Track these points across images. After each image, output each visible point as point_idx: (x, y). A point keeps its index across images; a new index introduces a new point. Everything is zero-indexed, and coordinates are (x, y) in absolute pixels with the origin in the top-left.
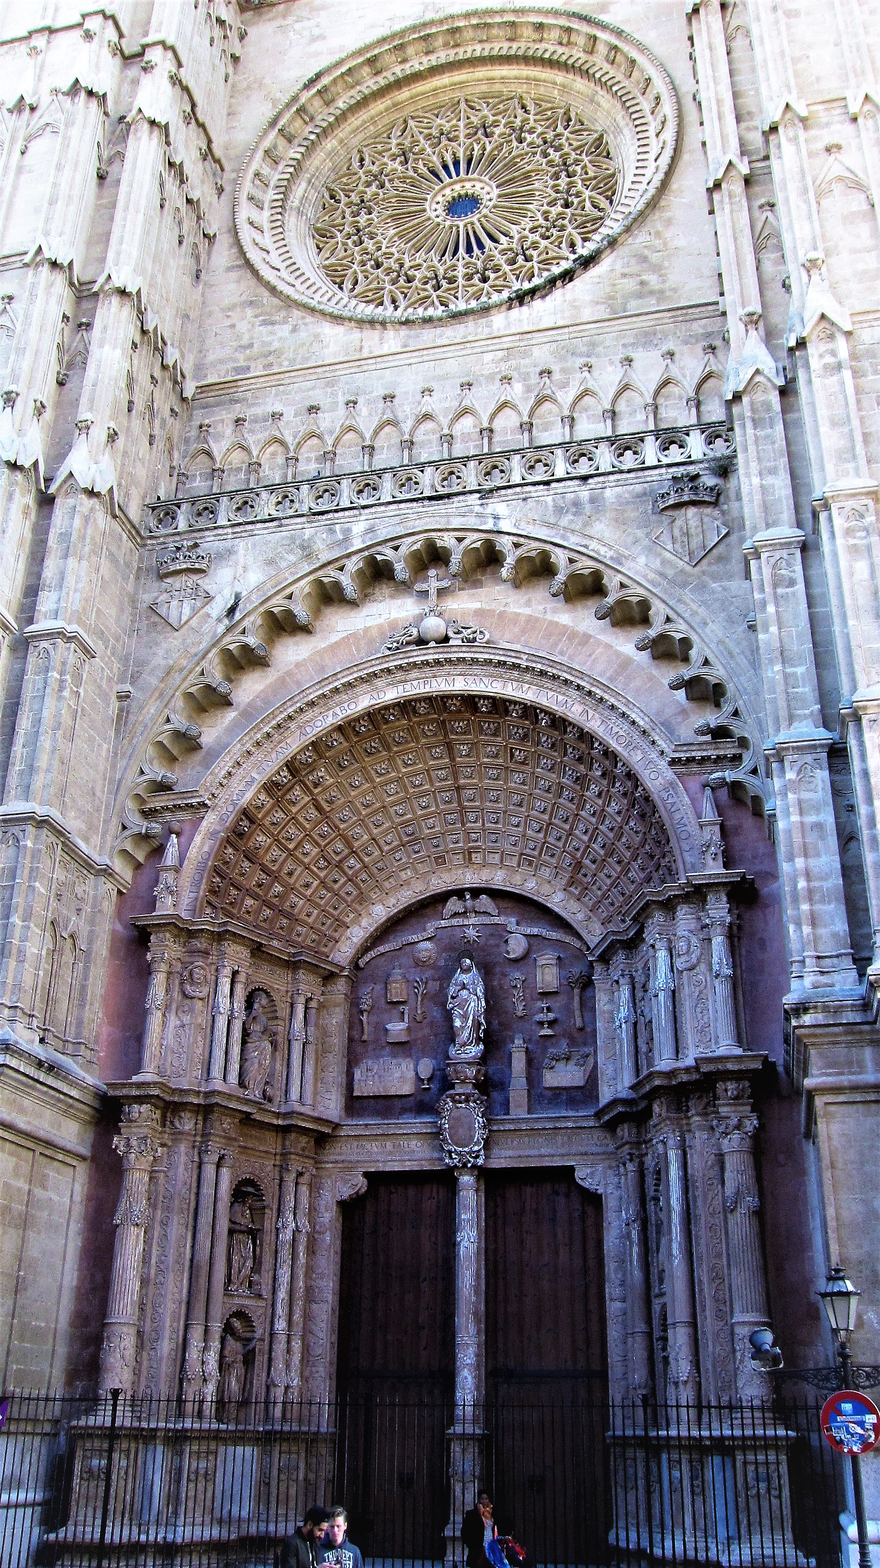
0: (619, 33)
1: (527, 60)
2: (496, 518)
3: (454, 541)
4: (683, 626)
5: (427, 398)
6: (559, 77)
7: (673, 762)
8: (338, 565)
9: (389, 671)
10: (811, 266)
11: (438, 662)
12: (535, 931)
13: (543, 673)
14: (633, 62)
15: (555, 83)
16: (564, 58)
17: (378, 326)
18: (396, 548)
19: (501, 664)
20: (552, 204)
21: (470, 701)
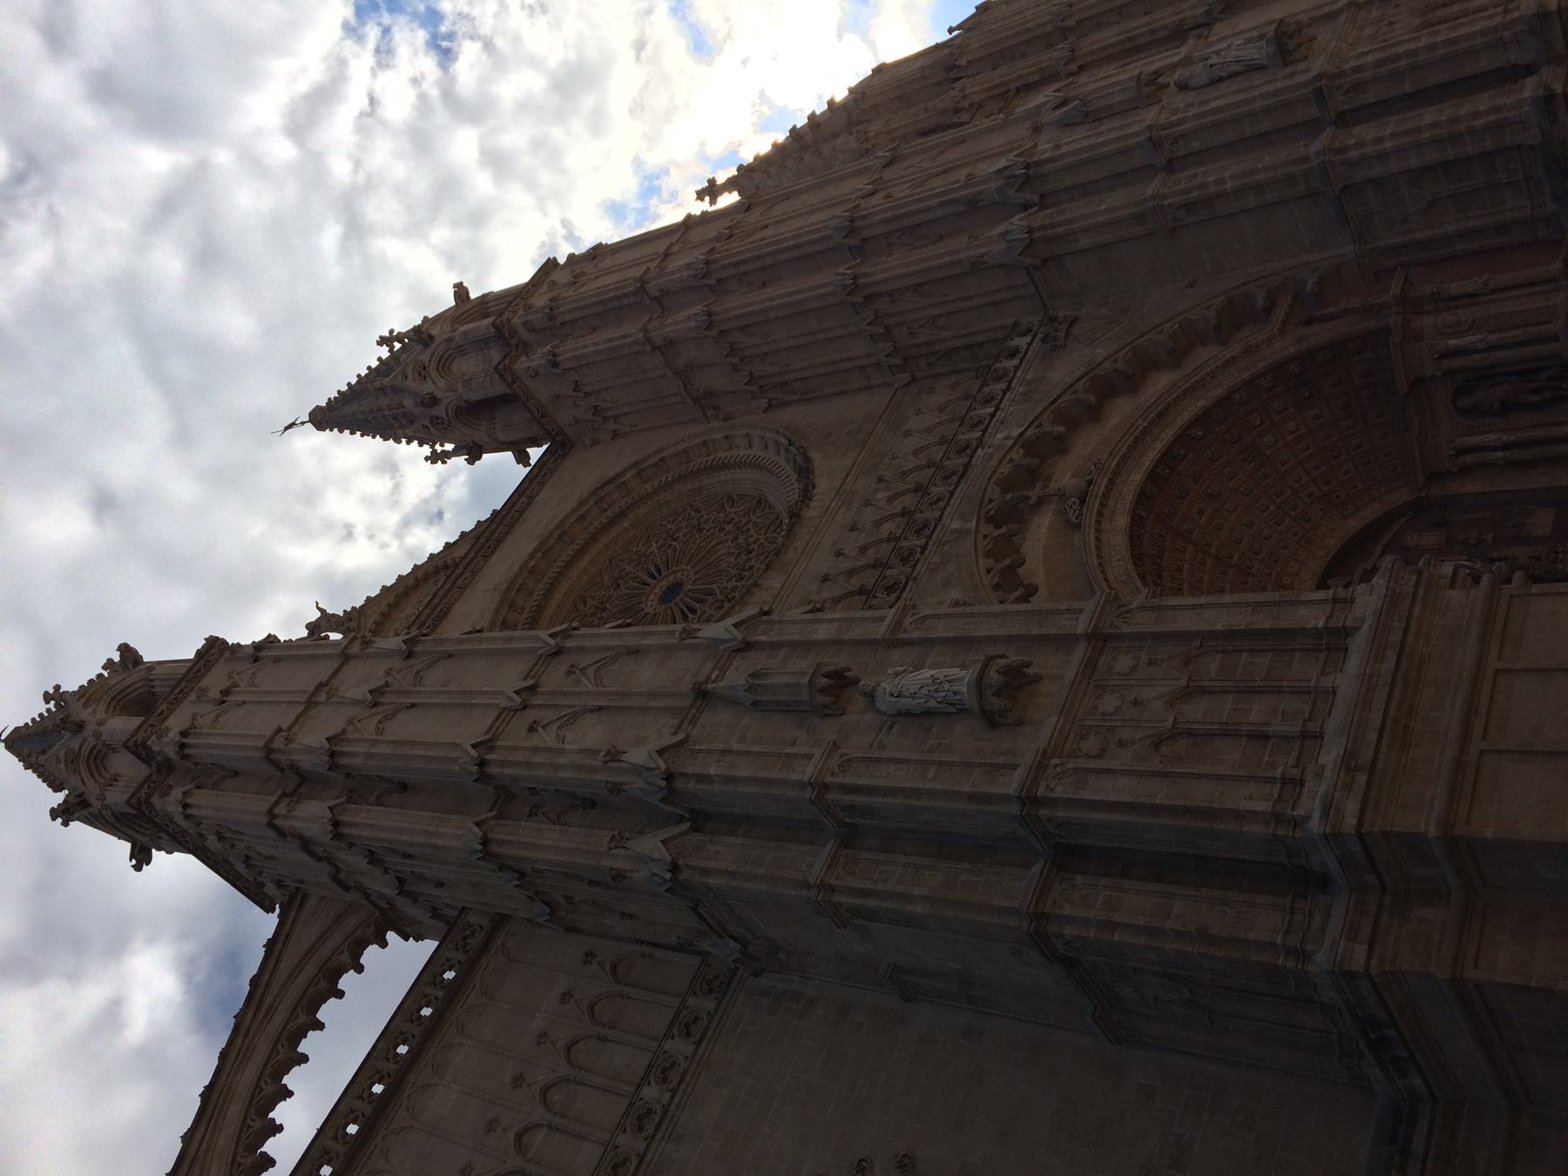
0: (636, 464)
1: (593, 538)
2: (1007, 438)
3: (1010, 465)
4: (1169, 325)
5: (846, 552)
6: (626, 525)
7: (1282, 332)
8: (980, 537)
9: (1100, 514)
10: (970, 176)
11: (1111, 483)
12: (1379, 549)
13: (1160, 415)
14: (662, 459)
15: (625, 529)
16: (617, 511)
17: (754, 589)
18: (991, 501)
19: (1136, 441)
20: (722, 530)
21: (1153, 476)
